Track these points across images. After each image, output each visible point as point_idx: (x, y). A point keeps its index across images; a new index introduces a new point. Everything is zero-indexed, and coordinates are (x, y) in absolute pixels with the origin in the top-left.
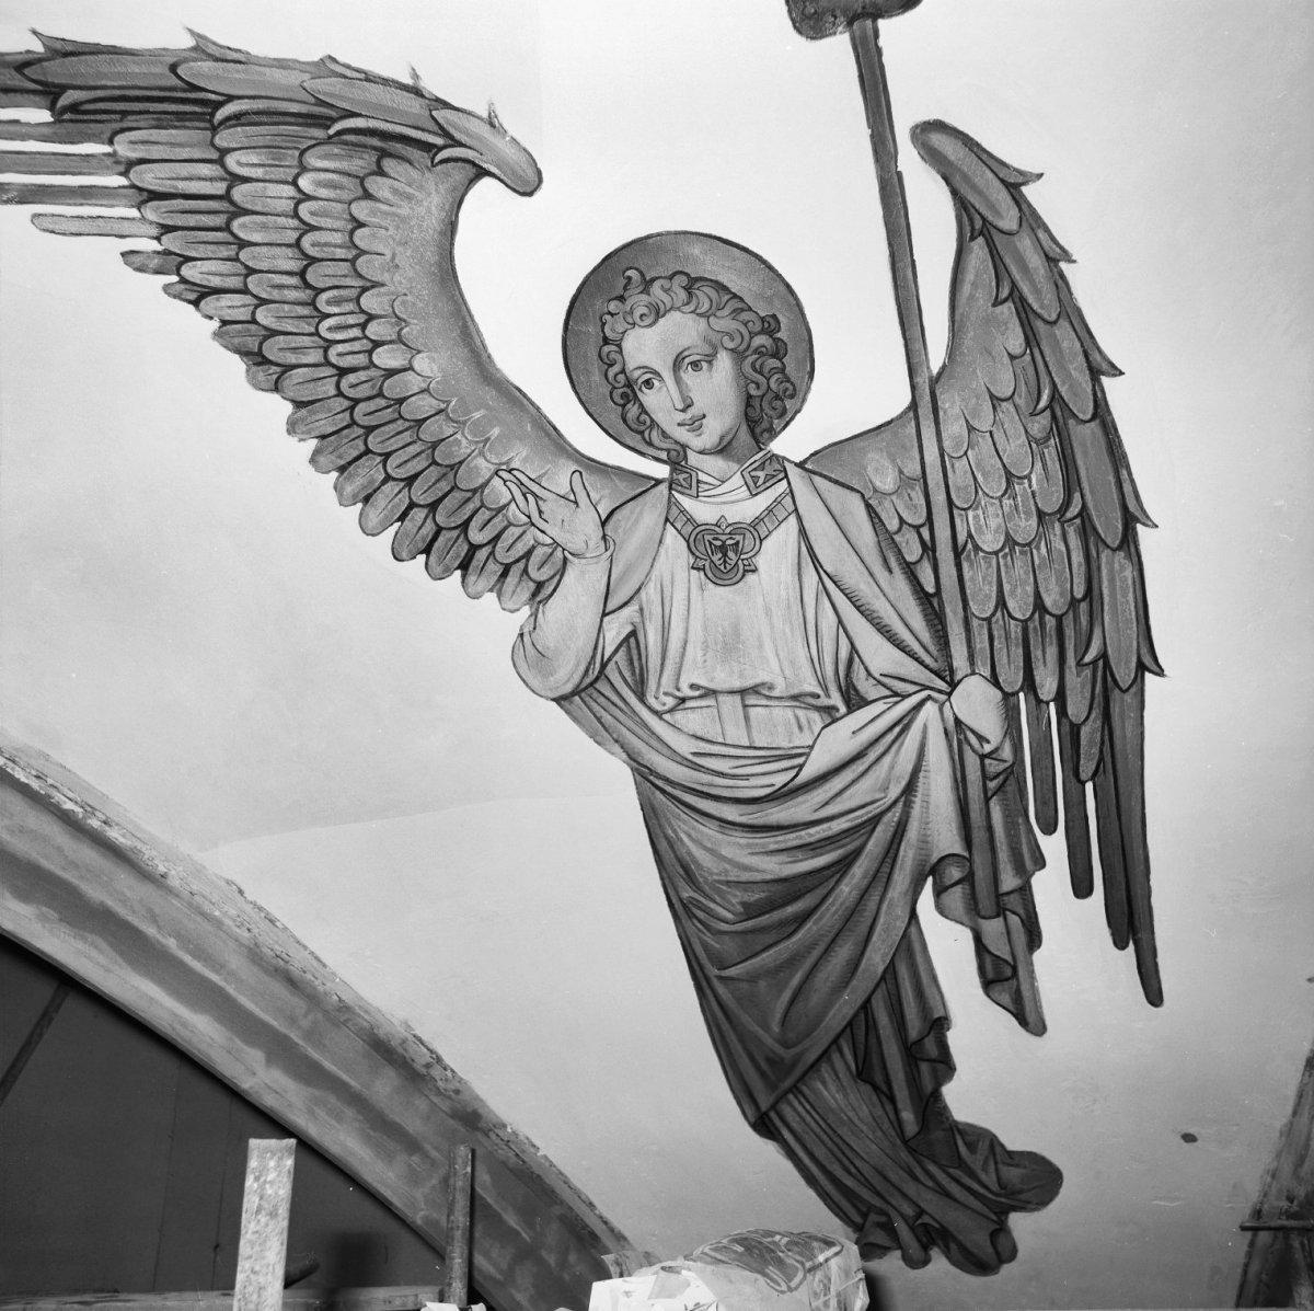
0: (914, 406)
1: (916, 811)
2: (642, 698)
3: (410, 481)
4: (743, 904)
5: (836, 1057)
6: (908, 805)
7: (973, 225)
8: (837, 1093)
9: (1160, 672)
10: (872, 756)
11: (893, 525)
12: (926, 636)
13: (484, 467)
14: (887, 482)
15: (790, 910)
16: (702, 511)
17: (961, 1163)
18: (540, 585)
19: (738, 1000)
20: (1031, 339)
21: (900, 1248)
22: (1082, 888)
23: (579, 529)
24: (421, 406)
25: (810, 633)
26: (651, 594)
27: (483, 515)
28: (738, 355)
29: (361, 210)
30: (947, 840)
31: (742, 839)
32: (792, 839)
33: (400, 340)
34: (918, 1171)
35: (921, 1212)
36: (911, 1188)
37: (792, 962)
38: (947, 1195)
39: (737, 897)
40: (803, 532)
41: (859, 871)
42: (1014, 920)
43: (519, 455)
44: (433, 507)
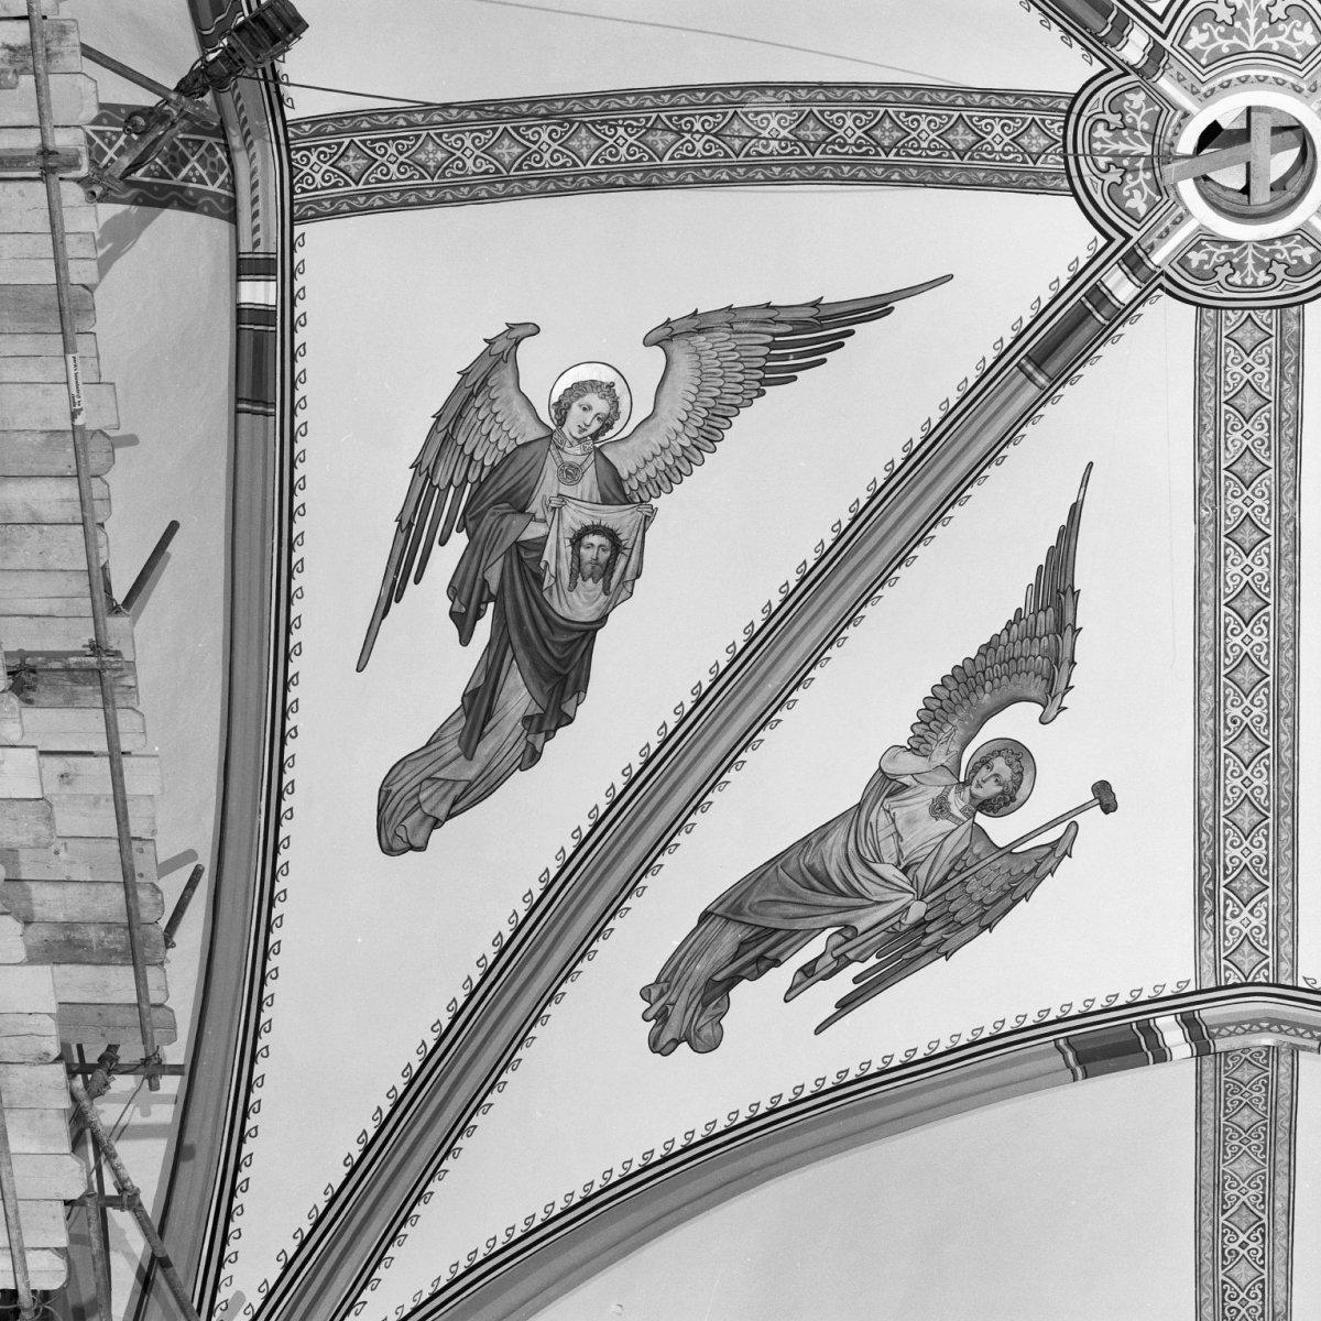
0: (1001, 849)
1: (871, 909)
2: (886, 797)
3: (950, 699)
4: (814, 864)
5: (749, 929)
6: (873, 905)
7: (1053, 846)
8: (732, 936)
9: (947, 959)
10: (887, 885)
11: (964, 858)
12: (934, 883)
13: (954, 722)
14: (976, 851)
15: (815, 883)
16: (951, 797)
17: (705, 1006)
18: (918, 749)
19: (768, 879)
20: (1028, 874)
21: (652, 1005)
22: (855, 980)
23: (940, 757)
24: (973, 699)
25: (923, 846)
26: (922, 788)
27: (940, 725)
28: (1003, 793)
29: (1032, 674)
30: (861, 926)
31: (842, 852)
32: (846, 871)
33: (993, 689)
34: (696, 991)
35: (673, 1004)
36: (685, 993)
37: (790, 892)
38: (687, 1010)
39: (817, 862)
40: (953, 831)
41: (840, 901)
42: (835, 964)
43: (960, 732)
44: (941, 708)
